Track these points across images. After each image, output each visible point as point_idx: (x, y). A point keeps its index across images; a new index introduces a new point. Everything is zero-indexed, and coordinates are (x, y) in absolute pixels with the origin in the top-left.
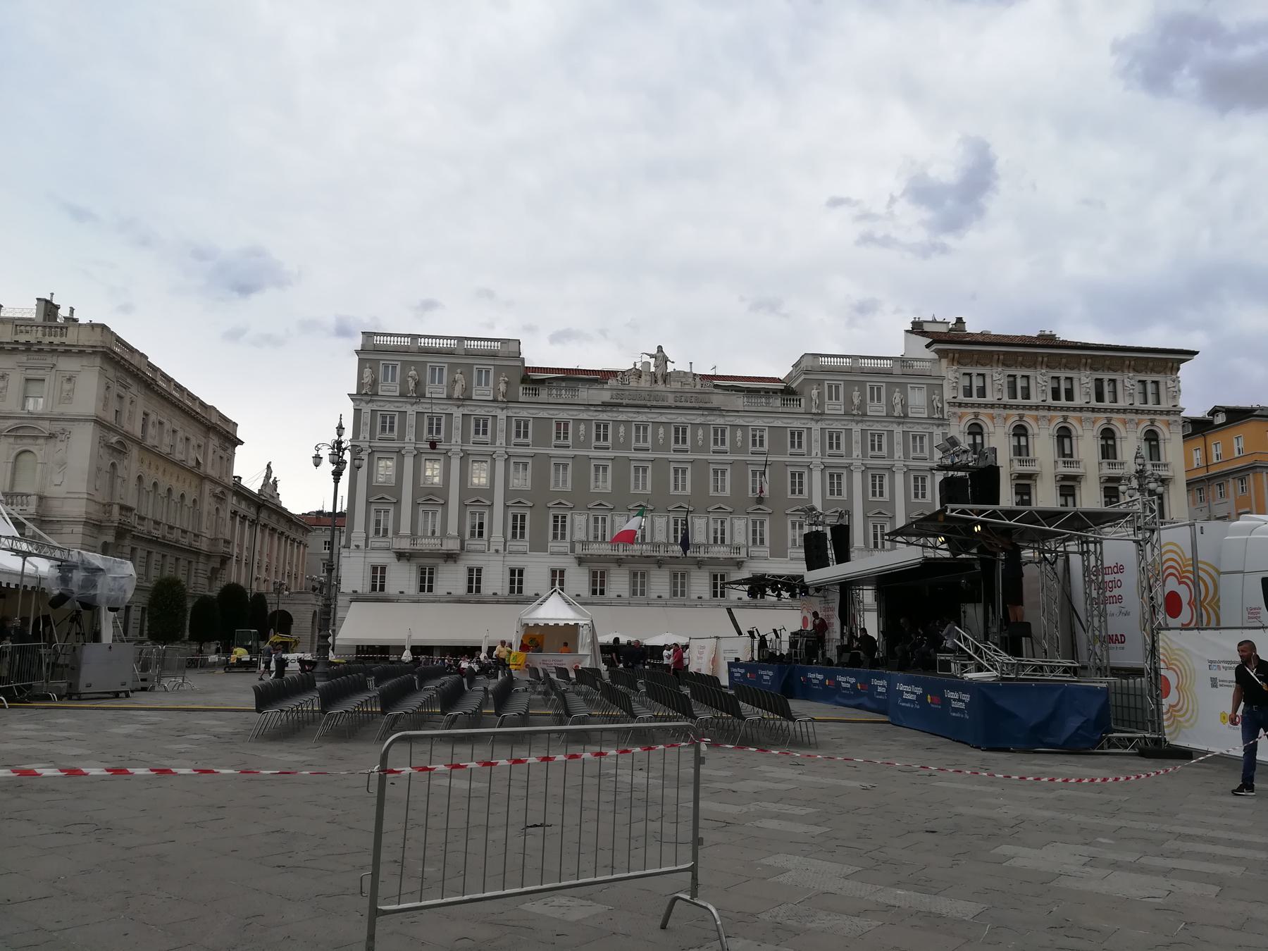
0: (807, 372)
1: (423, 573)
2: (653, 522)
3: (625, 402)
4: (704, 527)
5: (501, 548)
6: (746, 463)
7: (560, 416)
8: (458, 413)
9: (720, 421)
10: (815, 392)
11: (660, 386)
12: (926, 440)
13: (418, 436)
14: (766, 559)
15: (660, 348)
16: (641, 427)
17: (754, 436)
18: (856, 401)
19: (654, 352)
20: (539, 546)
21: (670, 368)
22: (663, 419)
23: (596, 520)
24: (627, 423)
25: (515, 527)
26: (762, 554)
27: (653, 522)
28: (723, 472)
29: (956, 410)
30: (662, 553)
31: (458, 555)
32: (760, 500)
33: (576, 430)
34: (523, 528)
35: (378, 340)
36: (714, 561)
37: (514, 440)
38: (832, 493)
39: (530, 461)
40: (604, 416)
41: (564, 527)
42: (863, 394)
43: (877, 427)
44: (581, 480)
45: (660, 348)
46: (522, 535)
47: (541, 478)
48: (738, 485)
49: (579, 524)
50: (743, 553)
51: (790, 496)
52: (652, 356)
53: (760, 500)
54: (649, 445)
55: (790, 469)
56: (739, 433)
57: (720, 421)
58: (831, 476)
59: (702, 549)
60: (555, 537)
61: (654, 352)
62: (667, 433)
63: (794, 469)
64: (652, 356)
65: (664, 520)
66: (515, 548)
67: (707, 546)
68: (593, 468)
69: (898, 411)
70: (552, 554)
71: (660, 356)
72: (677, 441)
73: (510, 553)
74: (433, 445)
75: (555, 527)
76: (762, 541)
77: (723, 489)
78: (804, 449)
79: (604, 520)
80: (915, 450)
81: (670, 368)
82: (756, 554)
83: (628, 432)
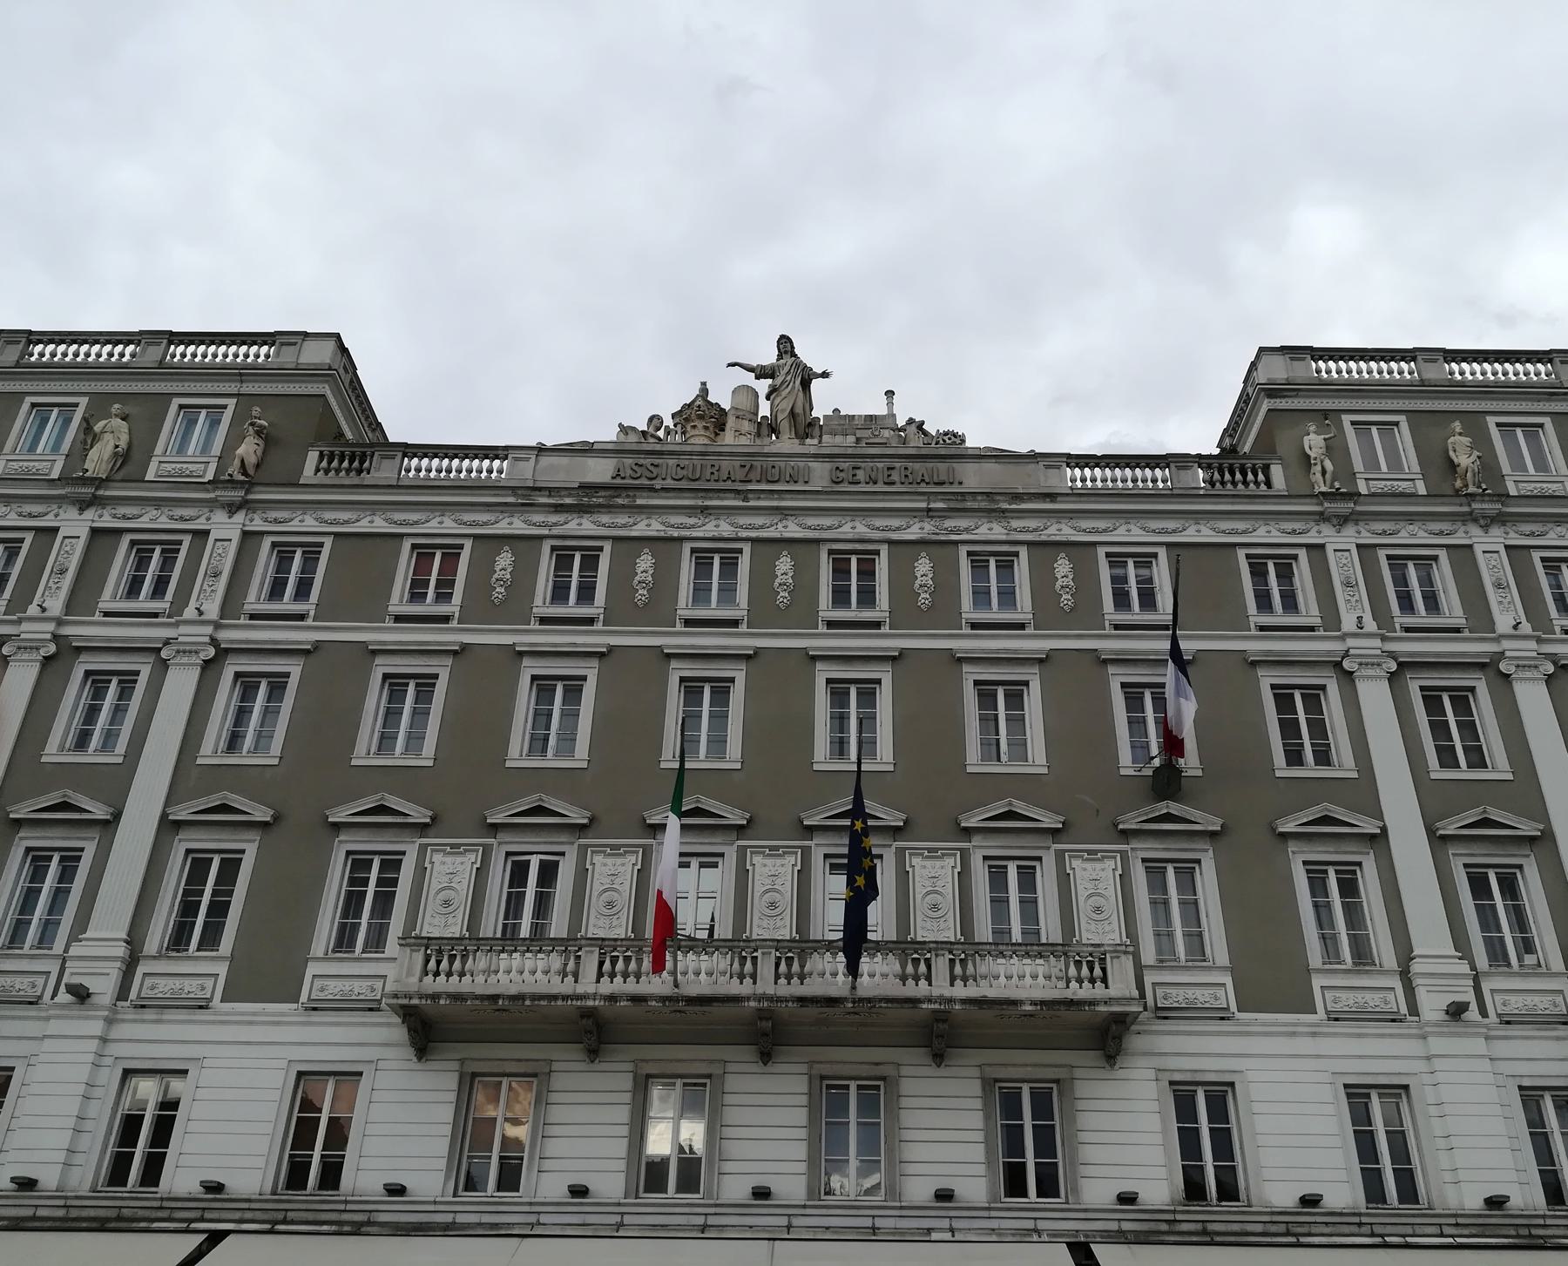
0: (1272, 392)
2: (743, 875)
3: (658, 484)
5: (104, 986)
6: (1103, 661)
7: (433, 526)
8: (75, 525)
10: (1314, 442)
11: (786, 443)
16: (715, 559)
17: (1119, 581)
18: (1464, 460)
19: (768, 355)
20: (267, 976)
21: (824, 399)
22: (792, 529)
23: (519, 873)
25: (188, 909)
27: (743, 875)
28: (1015, 698)
30: (766, 985)
33: (483, 567)
34: (219, 909)
36: (998, 1023)
38: (1447, 757)
39: (295, 669)
40: (584, 525)
41: (384, 902)
42: (1481, 441)
44: (476, 727)
46: (211, 937)
47: (325, 727)
48: (1079, 733)
49: (447, 883)
50: (1121, 982)
51: (1282, 770)
53: (1167, 782)
55: (1267, 680)
56: (1063, 567)
57: (991, 530)
58: (1432, 700)
59: (941, 965)
60: (344, 940)
61: (769, 356)
64: (761, 373)
66: (165, 987)
67: (965, 950)
71: (790, 372)
72: (840, 596)
75: (353, 903)
76: (1196, 941)
77: (1019, 748)
78: (1309, 612)
79: (548, 873)
81: (824, 399)
82: (1178, 997)
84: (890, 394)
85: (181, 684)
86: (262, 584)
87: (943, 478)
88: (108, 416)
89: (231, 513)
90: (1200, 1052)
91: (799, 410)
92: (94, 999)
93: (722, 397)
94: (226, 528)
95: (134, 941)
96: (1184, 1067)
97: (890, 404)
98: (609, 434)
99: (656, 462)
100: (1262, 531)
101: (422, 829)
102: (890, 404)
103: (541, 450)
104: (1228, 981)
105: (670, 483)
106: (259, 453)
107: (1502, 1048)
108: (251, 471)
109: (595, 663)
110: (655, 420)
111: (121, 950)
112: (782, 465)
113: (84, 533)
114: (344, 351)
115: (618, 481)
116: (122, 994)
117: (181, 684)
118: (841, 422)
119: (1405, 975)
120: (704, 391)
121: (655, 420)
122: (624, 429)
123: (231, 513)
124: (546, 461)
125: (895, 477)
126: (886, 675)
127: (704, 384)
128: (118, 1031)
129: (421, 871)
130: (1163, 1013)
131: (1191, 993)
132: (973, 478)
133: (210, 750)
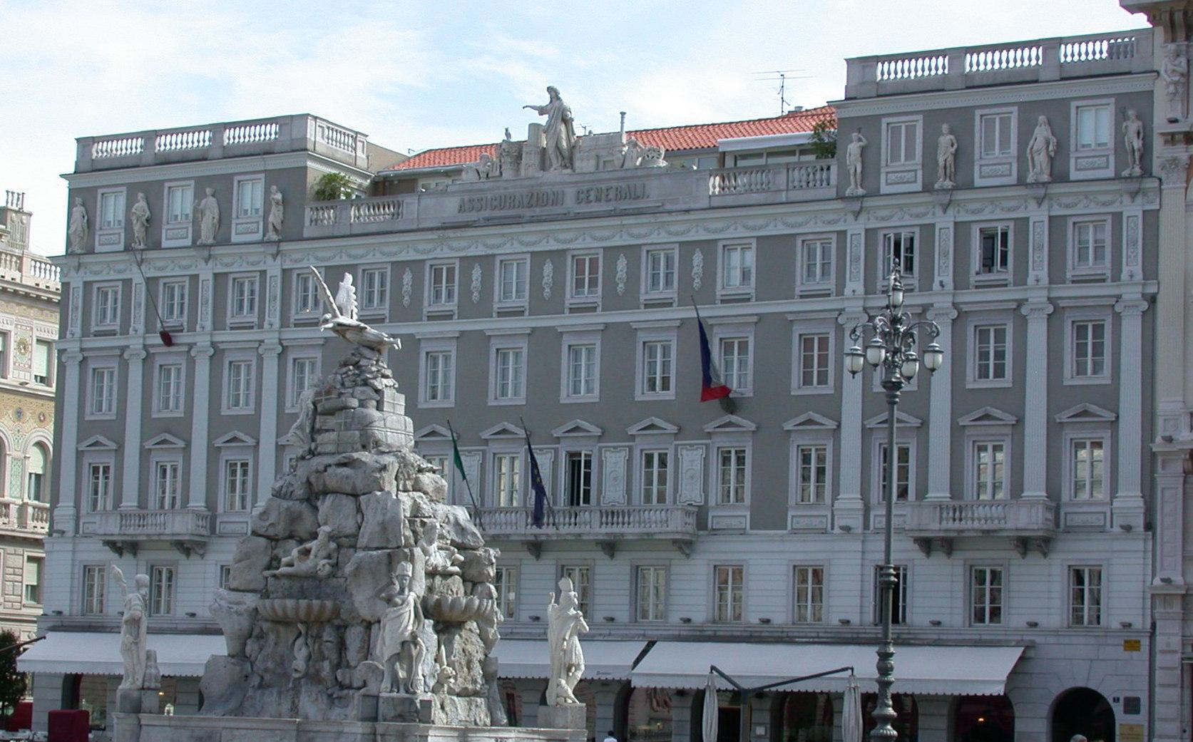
1: (1080, 580)
13: (149, 329)
14: (743, 532)
24: (416, 265)
26: (734, 523)
31: (203, 545)
35: (884, 72)
37: (293, 317)
54: (452, 306)
62: (559, 272)
63: (1079, 316)
65: (621, 457)
68: (423, 355)
69: (1040, 168)
74: (167, 339)
83: (559, 272)
88: (206, 196)
96: (719, 558)
106: (281, 214)
108: (279, 227)
130: (715, 531)
131: (728, 521)
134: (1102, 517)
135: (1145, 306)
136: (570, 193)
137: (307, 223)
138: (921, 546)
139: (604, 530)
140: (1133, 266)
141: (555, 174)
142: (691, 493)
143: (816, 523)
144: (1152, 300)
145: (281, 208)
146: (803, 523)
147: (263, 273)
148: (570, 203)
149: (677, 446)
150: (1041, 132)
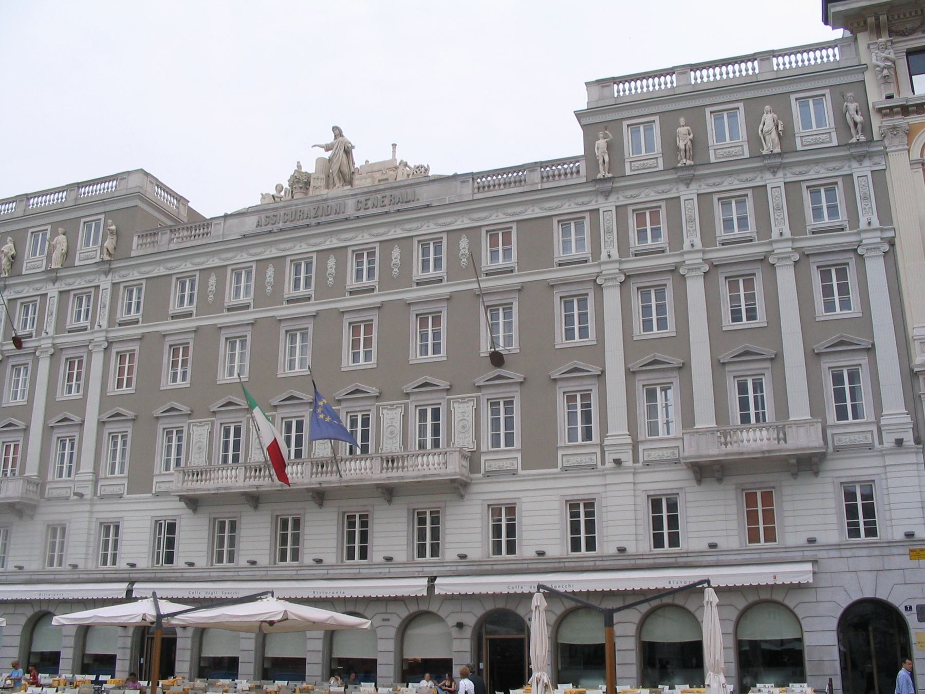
4: (398, 424)
8: (53, 291)
9: (430, 228)
12: (839, 192)
15: (337, 132)
19: (330, 138)
22: (334, 243)
29: (899, 120)
32: (497, 359)
39: (136, 347)
43: (729, 184)
45: (337, 132)
52: (328, 148)
61: (330, 138)
64: (328, 148)
69: (771, 144)
70: (157, 495)
73: (102, 497)
80: (817, 213)
81: (359, 160)
84: (394, 145)
85: (97, 360)
86: (122, 307)
87: (409, 198)
89: (106, 276)
90: (501, 491)
91: (346, 170)
92: (85, 497)
93: (310, 167)
94: (105, 283)
95: (96, 472)
97: (394, 152)
98: (256, 201)
99: (275, 213)
100: (566, 206)
101: (189, 416)
102: (394, 152)
103: (226, 216)
104: (519, 456)
105: (281, 225)
106: (114, 242)
107: (641, 478)
108: (112, 252)
109: (250, 328)
110: (279, 188)
111: (90, 477)
112: (333, 204)
113: (56, 294)
114: (147, 174)
115: (260, 230)
116: (95, 493)
117: (97, 360)
118: (371, 169)
119: (602, 446)
120: (299, 166)
121: (279, 188)
122: (264, 197)
123: (106, 276)
124: (230, 221)
125: (387, 201)
126: (375, 317)
127: (298, 162)
128: (96, 508)
129: (189, 434)
132: (425, 195)
133: (112, 390)
134: (869, 436)
135: (886, 247)
136: (351, 203)
137: (134, 246)
138: (695, 472)
139: (385, 475)
140: (868, 215)
141: (340, 190)
142: (464, 440)
143: (585, 460)
144: (892, 244)
145: (115, 237)
146: (573, 461)
147: (97, 287)
148: (350, 211)
149: (449, 400)
150: (768, 119)
